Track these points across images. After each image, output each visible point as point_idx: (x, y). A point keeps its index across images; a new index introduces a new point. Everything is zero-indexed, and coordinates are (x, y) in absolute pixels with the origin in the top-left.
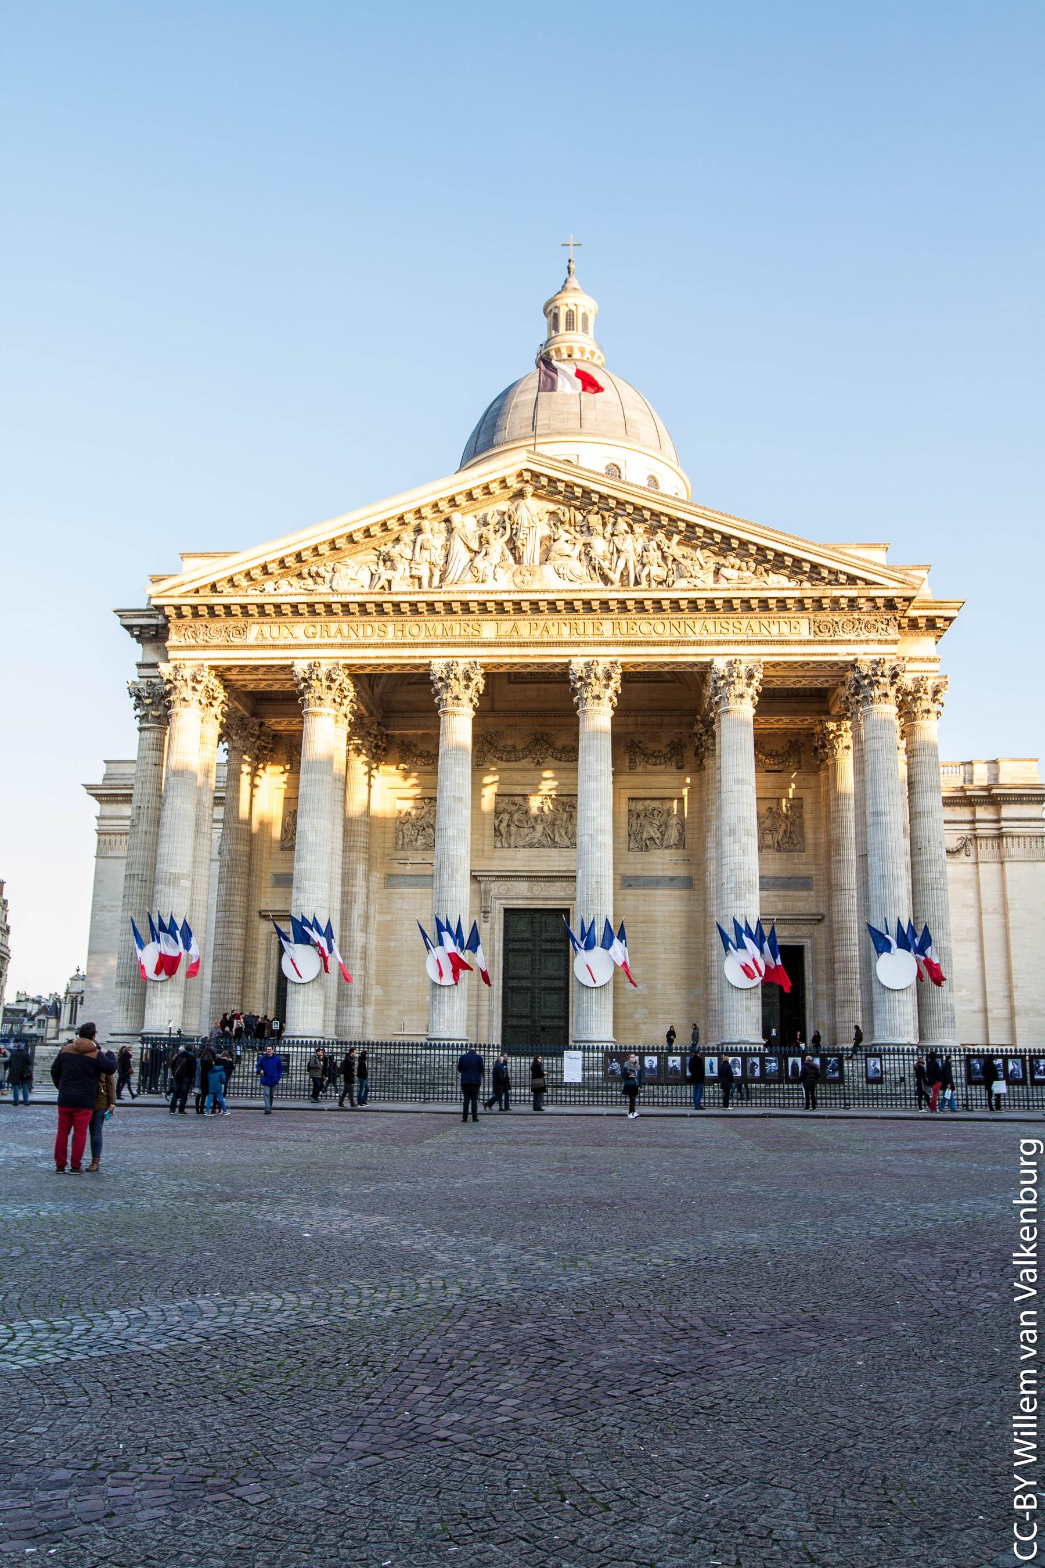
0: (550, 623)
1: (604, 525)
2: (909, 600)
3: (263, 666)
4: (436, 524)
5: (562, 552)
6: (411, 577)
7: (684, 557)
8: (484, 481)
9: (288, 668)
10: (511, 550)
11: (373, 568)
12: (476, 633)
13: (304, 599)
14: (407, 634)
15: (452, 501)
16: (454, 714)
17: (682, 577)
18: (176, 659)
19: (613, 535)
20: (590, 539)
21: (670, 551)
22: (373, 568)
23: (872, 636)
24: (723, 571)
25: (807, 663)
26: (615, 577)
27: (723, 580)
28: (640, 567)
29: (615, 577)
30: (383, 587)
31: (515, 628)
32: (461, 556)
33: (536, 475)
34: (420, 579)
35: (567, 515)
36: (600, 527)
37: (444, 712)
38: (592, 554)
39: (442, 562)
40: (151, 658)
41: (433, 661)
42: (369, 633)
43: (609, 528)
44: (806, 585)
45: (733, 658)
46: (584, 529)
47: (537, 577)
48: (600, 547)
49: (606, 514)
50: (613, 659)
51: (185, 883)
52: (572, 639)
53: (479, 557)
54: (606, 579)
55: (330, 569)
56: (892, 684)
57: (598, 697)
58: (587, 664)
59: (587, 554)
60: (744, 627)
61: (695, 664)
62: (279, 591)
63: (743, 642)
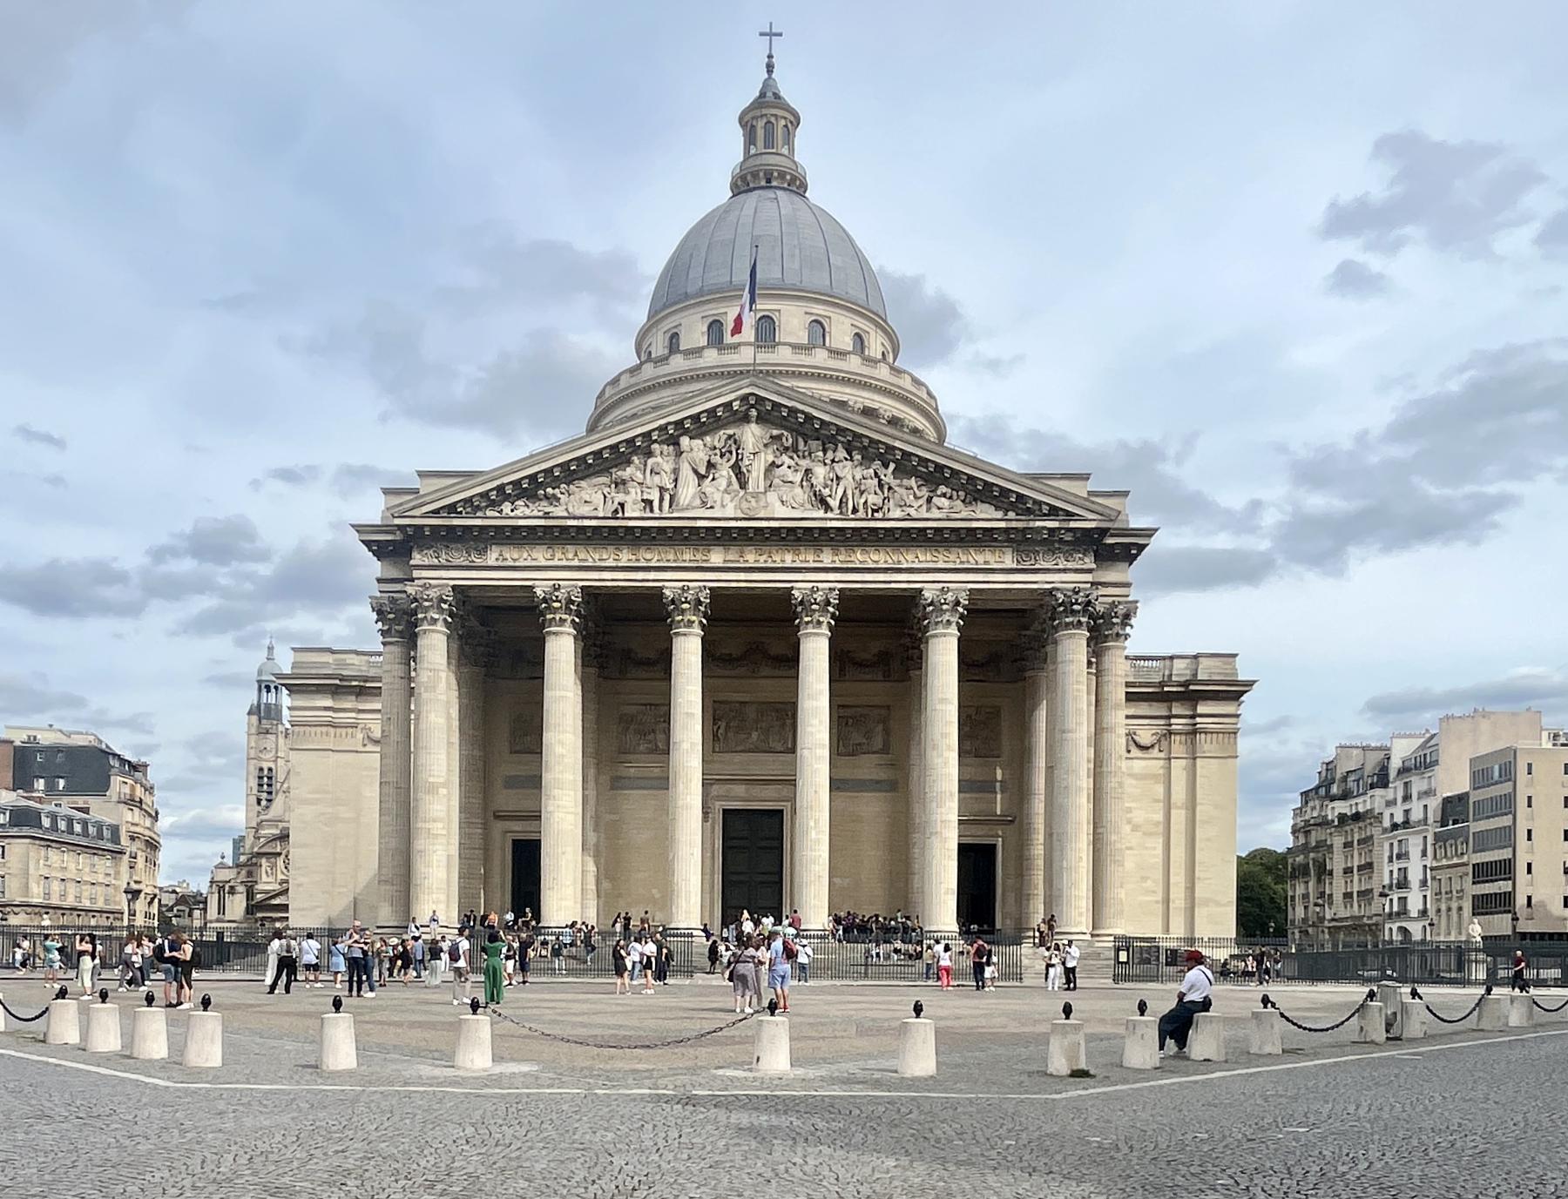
1: (825, 451)
2: (1104, 532)
13: (542, 522)
23: (1070, 565)
24: (935, 500)
27: (934, 510)
29: (834, 503)
30: (616, 511)
34: (651, 502)
38: (814, 481)
43: (830, 455)
44: (1011, 515)
48: (820, 472)
51: (443, 791)
54: (828, 508)
56: (1085, 611)
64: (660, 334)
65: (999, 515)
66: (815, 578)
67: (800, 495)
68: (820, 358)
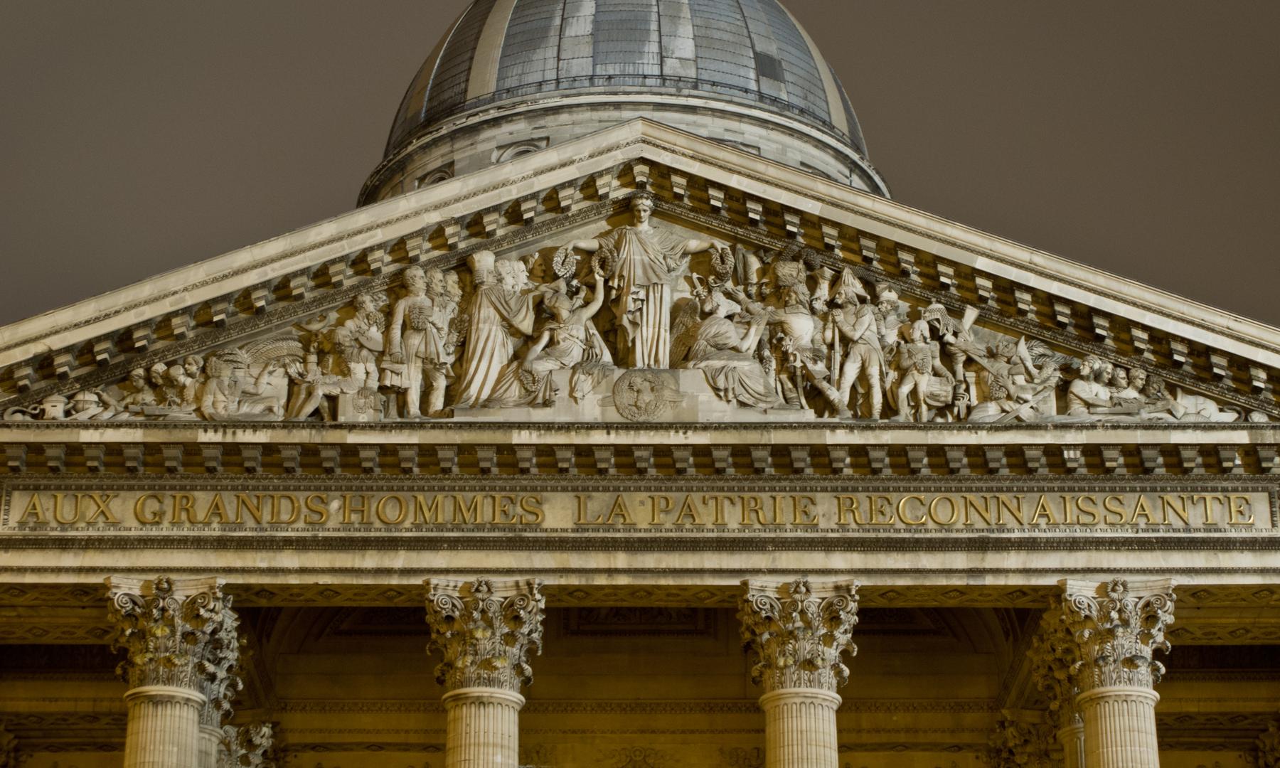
0: (696, 497)
3: (35, 586)
4: (438, 275)
5: (721, 341)
6: (382, 389)
7: (992, 355)
8: (545, 183)
9: (96, 596)
10: (605, 335)
12: (531, 518)
13: (136, 436)
14: (374, 519)
15: (474, 224)
16: (480, 702)
17: (985, 398)
19: (832, 304)
20: (781, 315)
22: (295, 369)
24: (1079, 387)
28: (893, 375)
29: (840, 396)
30: (317, 412)
31: (618, 509)
32: (493, 349)
33: (662, 173)
34: (401, 393)
35: (731, 260)
36: (803, 288)
37: (457, 698)
38: (789, 345)
39: (452, 359)
41: (434, 580)
42: (285, 517)
43: (823, 291)
44: (1258, 417)
45: (1108, 578)
47: (667, 394)
48: (803, 328)
49: (817, 259)
50: (842, 580)
52: (747, 534)
57: (810, 664)
58: (784, 589)
60: (1127, 513)
61: (1021, 591)
65: (1230, 417)
66: (805, 569)
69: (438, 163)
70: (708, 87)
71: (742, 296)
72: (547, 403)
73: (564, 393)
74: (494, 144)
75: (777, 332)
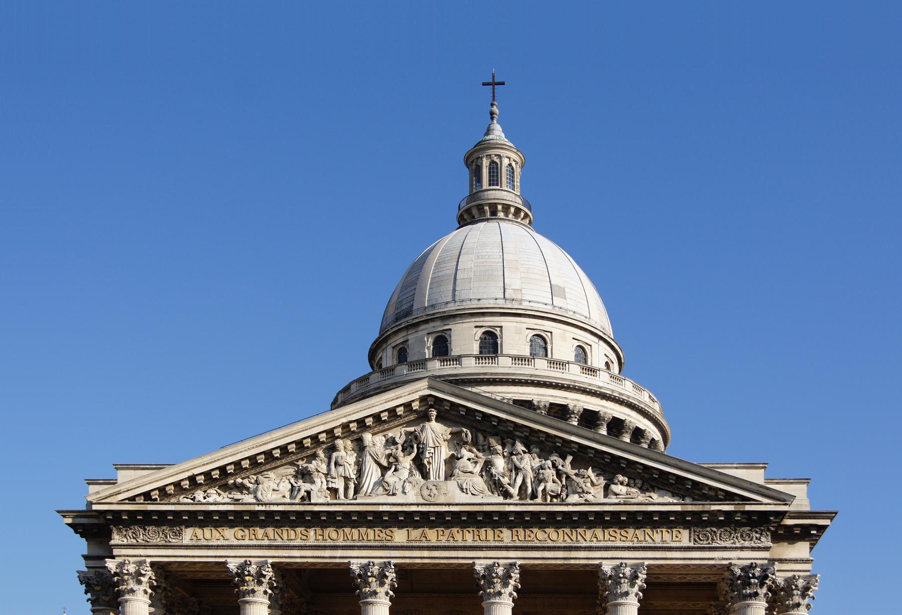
4: (349, 443)
7: (576, 475)
11: (292, 481)
17: (575, 492)
18: (120, 556)
21: (564, 469)
25: (688, 566)
26: (514, 491)
29: (514, 491)
30: (303, 498)
36: (499, 448)
38: (493, 471)
40: (98, 552)
46: (486, 447)
47: (443, 491)
48: (500, 464)
53: (390, 473)
54: (507, 495)
55: (253, 481)
59: (488, 472)
62: (208, 499)
63: (628, 549)
64: (389, 351)
67: (480, 482)
68: (540, 368)
69: (401, 340)
70: (527, 304)
71: (475, 450)
72: (394, 494)
73: (401, 490)
74: (426, 332)
75: (488, 465)
